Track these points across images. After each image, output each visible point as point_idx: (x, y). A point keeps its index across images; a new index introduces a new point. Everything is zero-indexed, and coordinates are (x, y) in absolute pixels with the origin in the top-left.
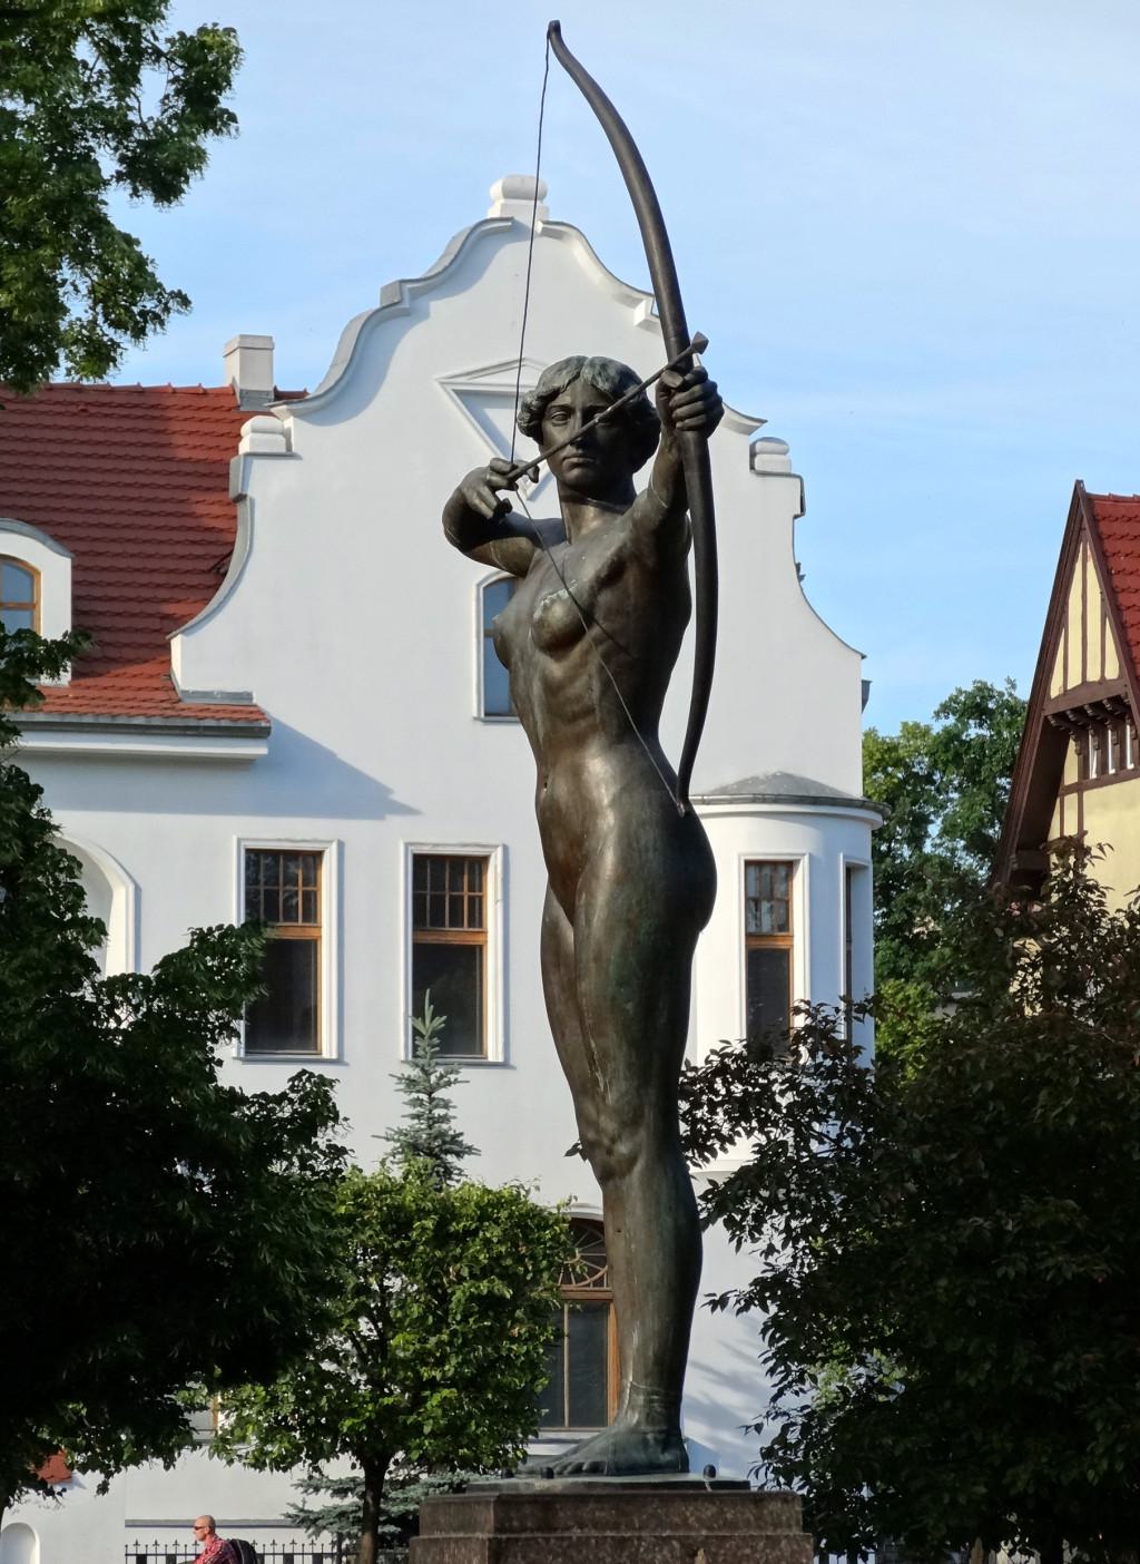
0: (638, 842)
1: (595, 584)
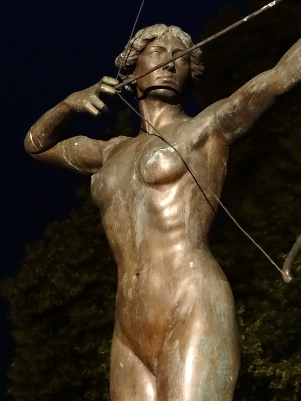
0: (216, 311)
1: (189, 147)
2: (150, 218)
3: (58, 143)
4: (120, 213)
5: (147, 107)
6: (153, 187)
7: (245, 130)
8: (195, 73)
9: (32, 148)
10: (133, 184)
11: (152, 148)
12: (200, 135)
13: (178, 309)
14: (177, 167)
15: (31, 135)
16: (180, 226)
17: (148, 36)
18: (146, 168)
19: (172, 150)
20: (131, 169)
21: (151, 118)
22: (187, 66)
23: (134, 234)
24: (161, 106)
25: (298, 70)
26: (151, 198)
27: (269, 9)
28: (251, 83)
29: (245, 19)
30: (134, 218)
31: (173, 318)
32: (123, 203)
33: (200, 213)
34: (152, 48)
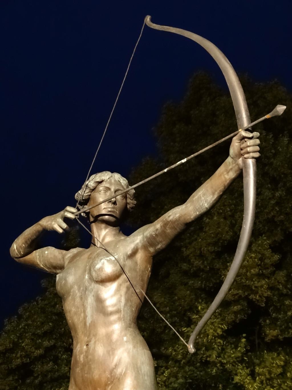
0: (141, 372)
1: (125, 257)
2: (97, 306)
3: (33, 251)
4: (76, 302)
5: (97, 228)
6: (99, 284)
7: (164, 246)
8: (130, 206)
9: (15, 254)
10: (85, 281)
11: (99, 257)
12: (133, 249)
13: (115, 370)
14: (116, 271)
15: (15, 245)
16: (118, 311)
17: (98, 180)
18: (95, 271)
19: (113, 259)
20: (85, 271)
21: (99, 236)
22: (124, 201)
23: (85, 317)
24: (106, 228)
25: (201, 206)
26: (98, 291)
27: (182, 164)
28: (169, 214)
29: (166, 170)
30: (86, 305)
31: (111, 376)
32: (78, 294)
33: (131, 303)
34: (101, 188)
